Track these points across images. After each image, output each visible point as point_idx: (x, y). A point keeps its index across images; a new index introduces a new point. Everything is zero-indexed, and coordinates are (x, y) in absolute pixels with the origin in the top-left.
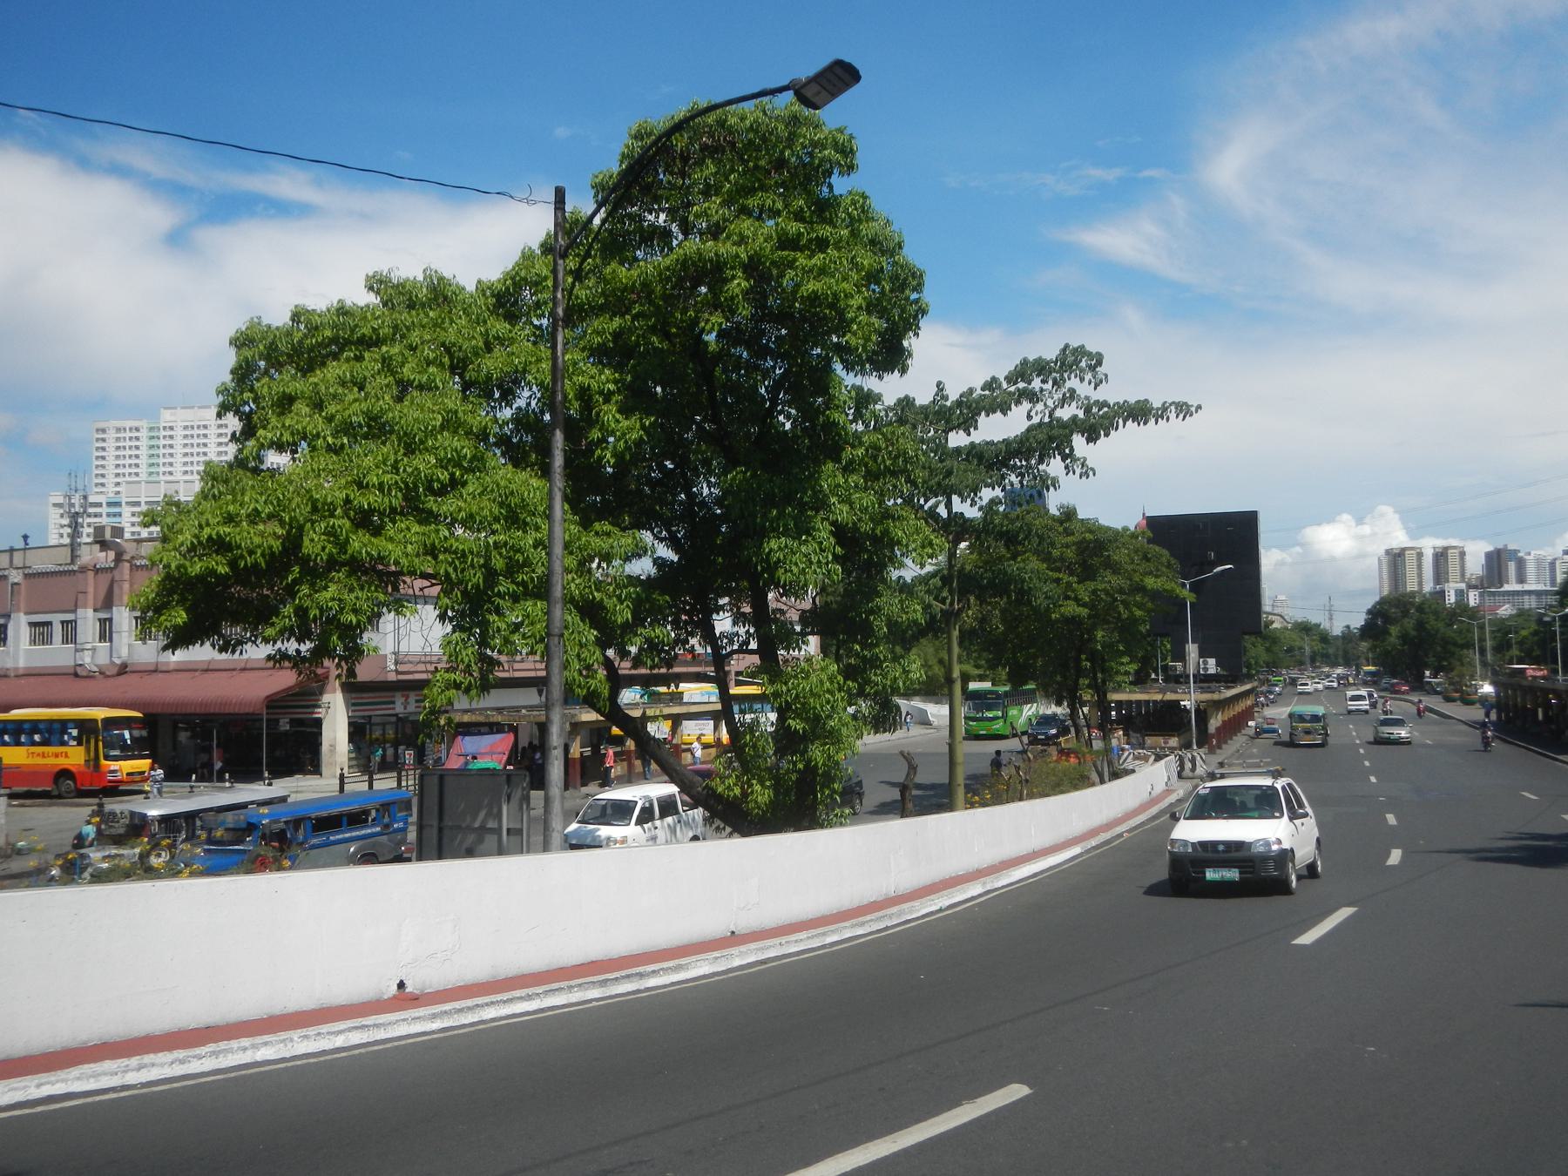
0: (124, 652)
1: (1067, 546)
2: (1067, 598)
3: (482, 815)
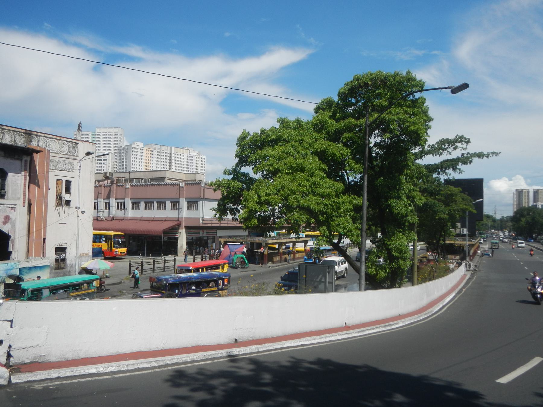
0: (114, 213)
3: (320, 276)
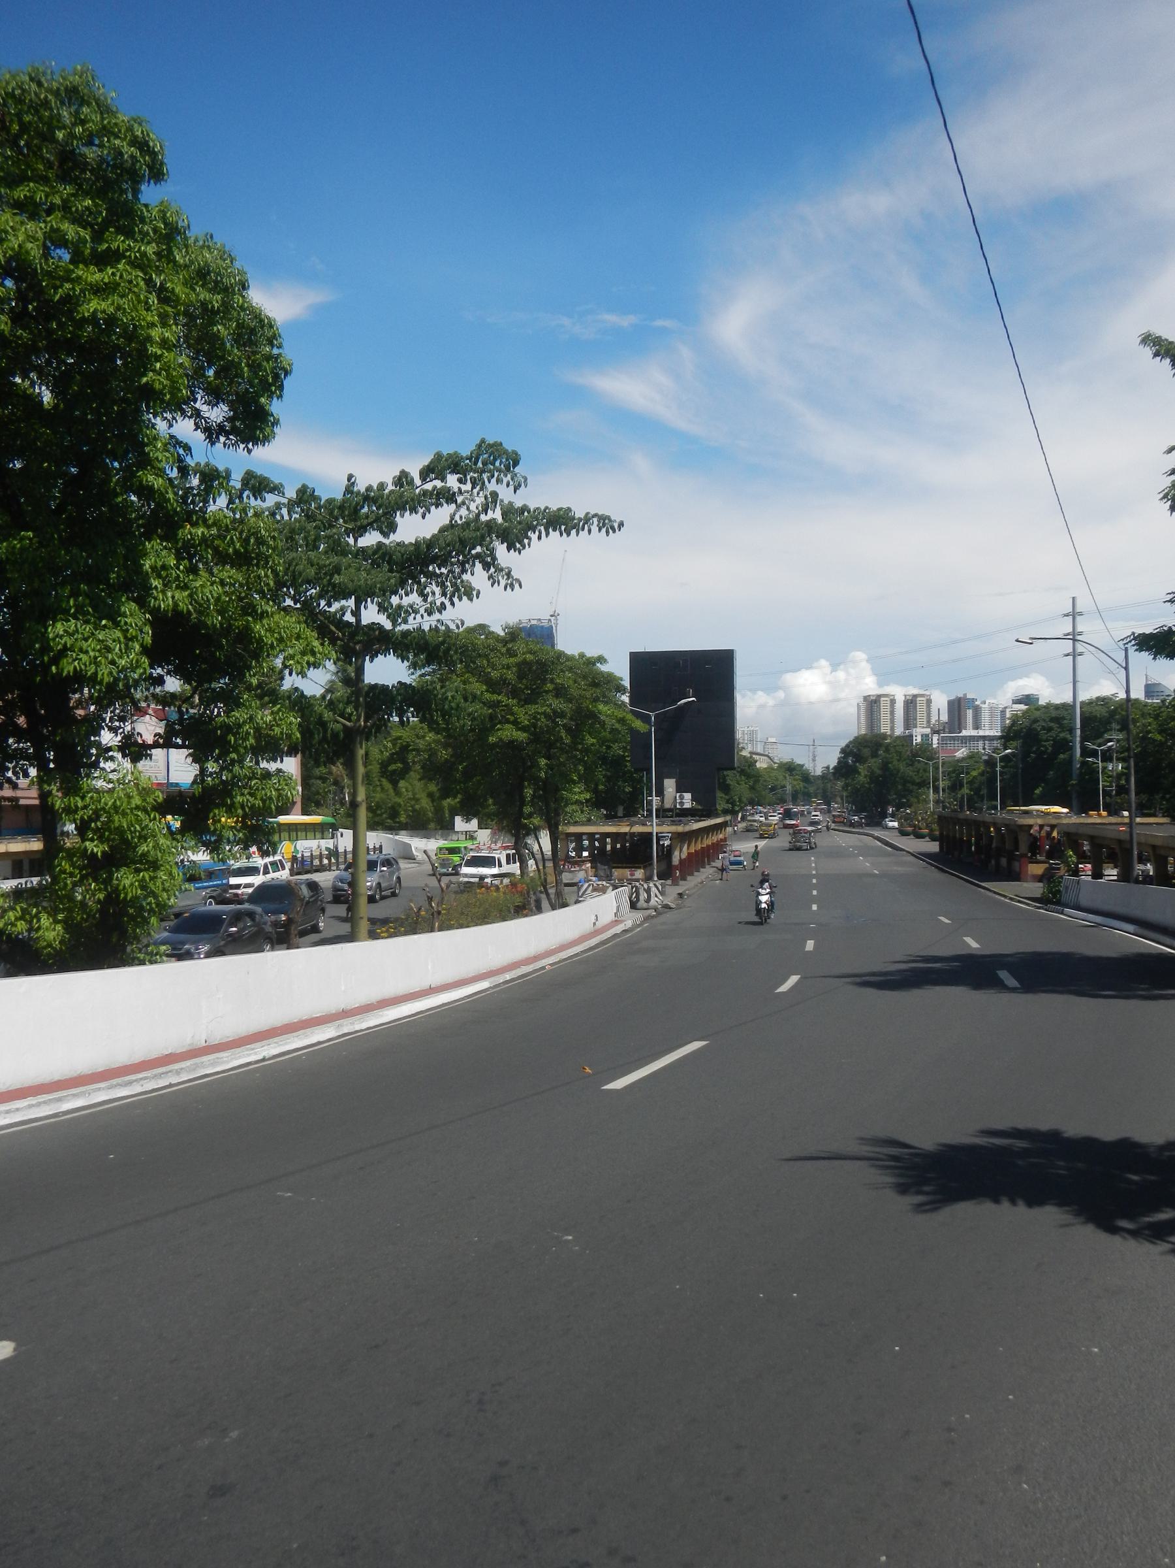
1: (508, 668)
2: (508, 721)
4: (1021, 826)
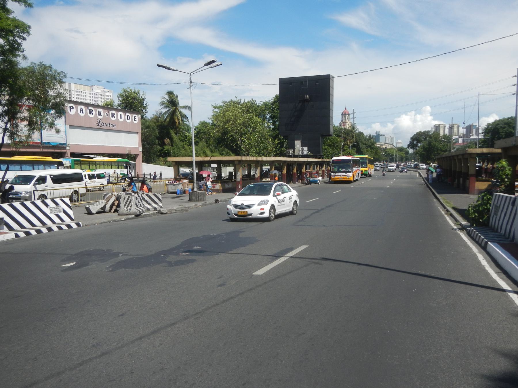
4: (471, 154)
